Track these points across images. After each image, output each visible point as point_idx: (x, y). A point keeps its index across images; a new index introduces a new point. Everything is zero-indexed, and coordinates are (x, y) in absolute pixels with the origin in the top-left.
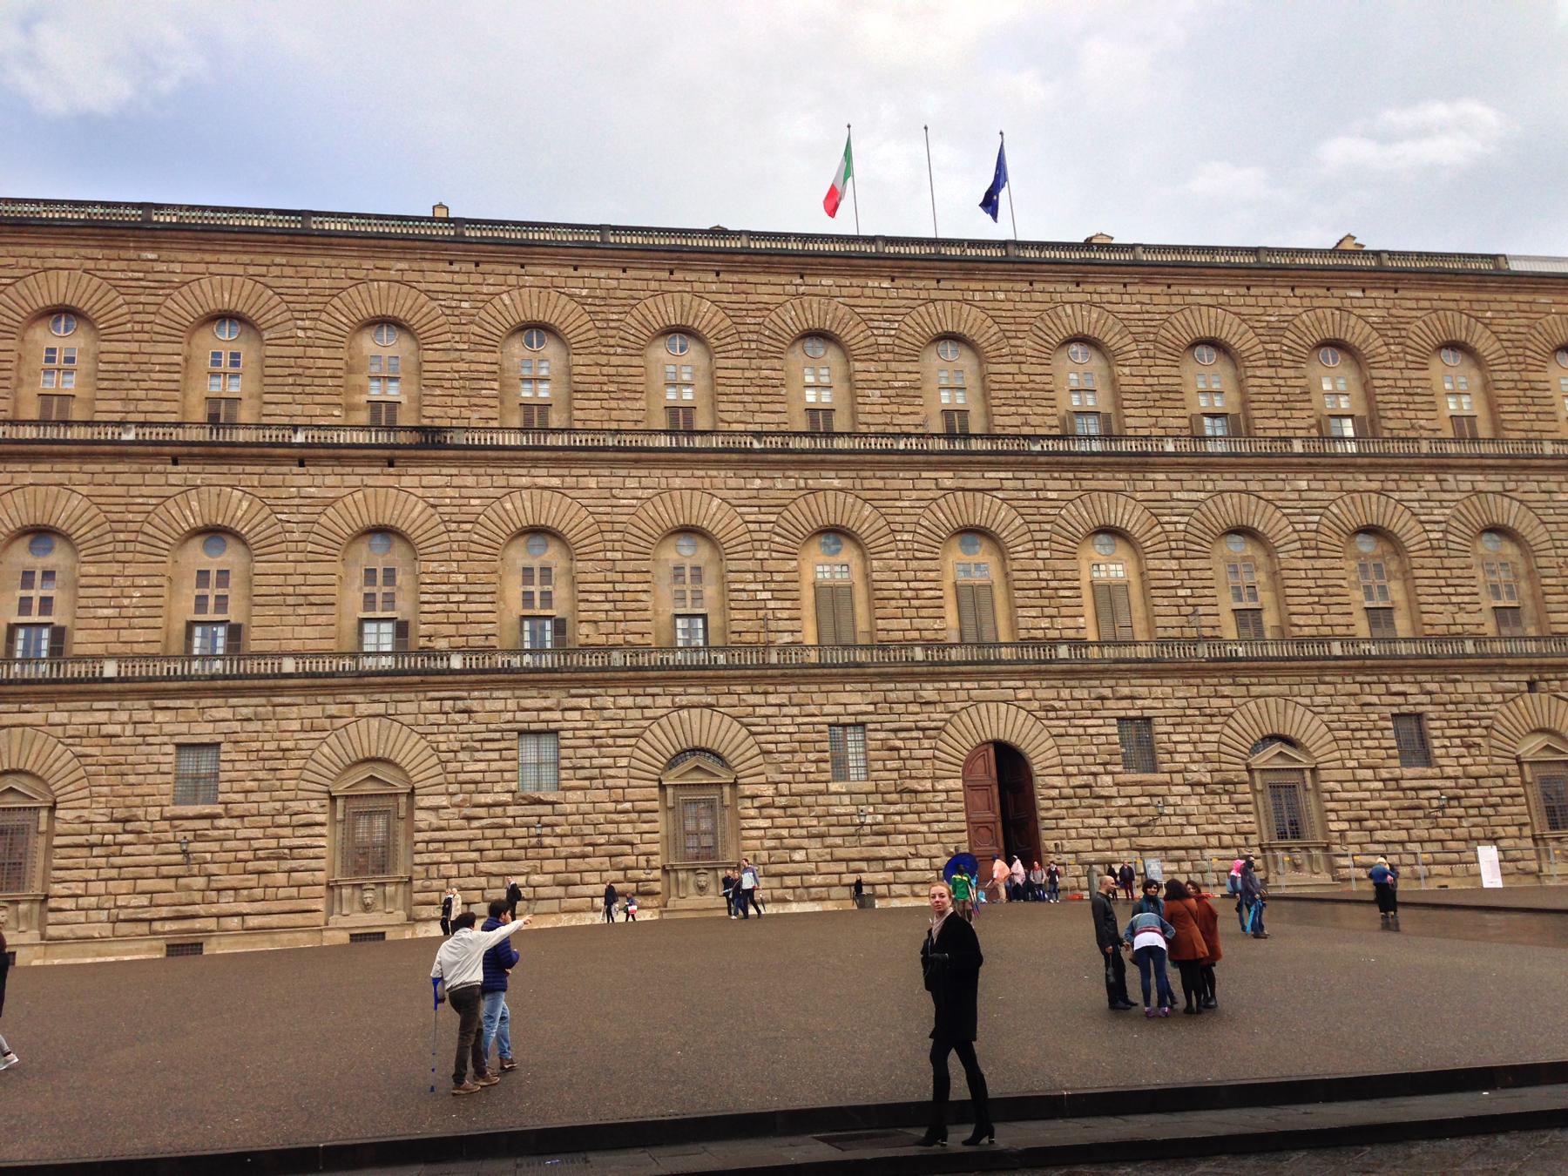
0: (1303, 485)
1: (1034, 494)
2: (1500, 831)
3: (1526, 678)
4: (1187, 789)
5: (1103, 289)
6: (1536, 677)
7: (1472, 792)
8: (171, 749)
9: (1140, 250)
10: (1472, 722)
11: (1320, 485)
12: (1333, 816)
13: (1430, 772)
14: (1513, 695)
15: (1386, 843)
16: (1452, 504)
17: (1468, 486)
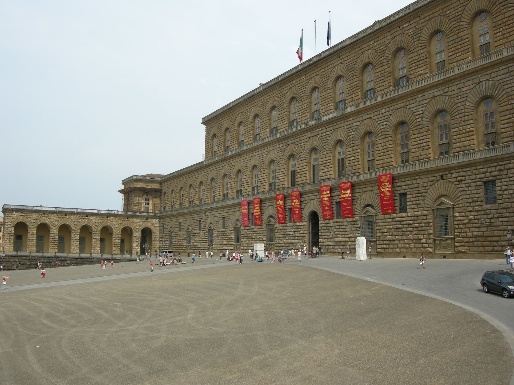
0: (383, 111)
1: (324, 134)
2: (421, 237)
3: (440, 174)
4: (346, 223)
5: (344, 56)
6: (443, 174)
7: (415, 222)
8: (222, 218)
9: (323, 54)
10: (419, 195)
11: (388, 109)
12: (378, 232)
13: (404, 214)
14: (433, 182)
15: (390, 240)
16: (425, 105)
17: (431, 96)
